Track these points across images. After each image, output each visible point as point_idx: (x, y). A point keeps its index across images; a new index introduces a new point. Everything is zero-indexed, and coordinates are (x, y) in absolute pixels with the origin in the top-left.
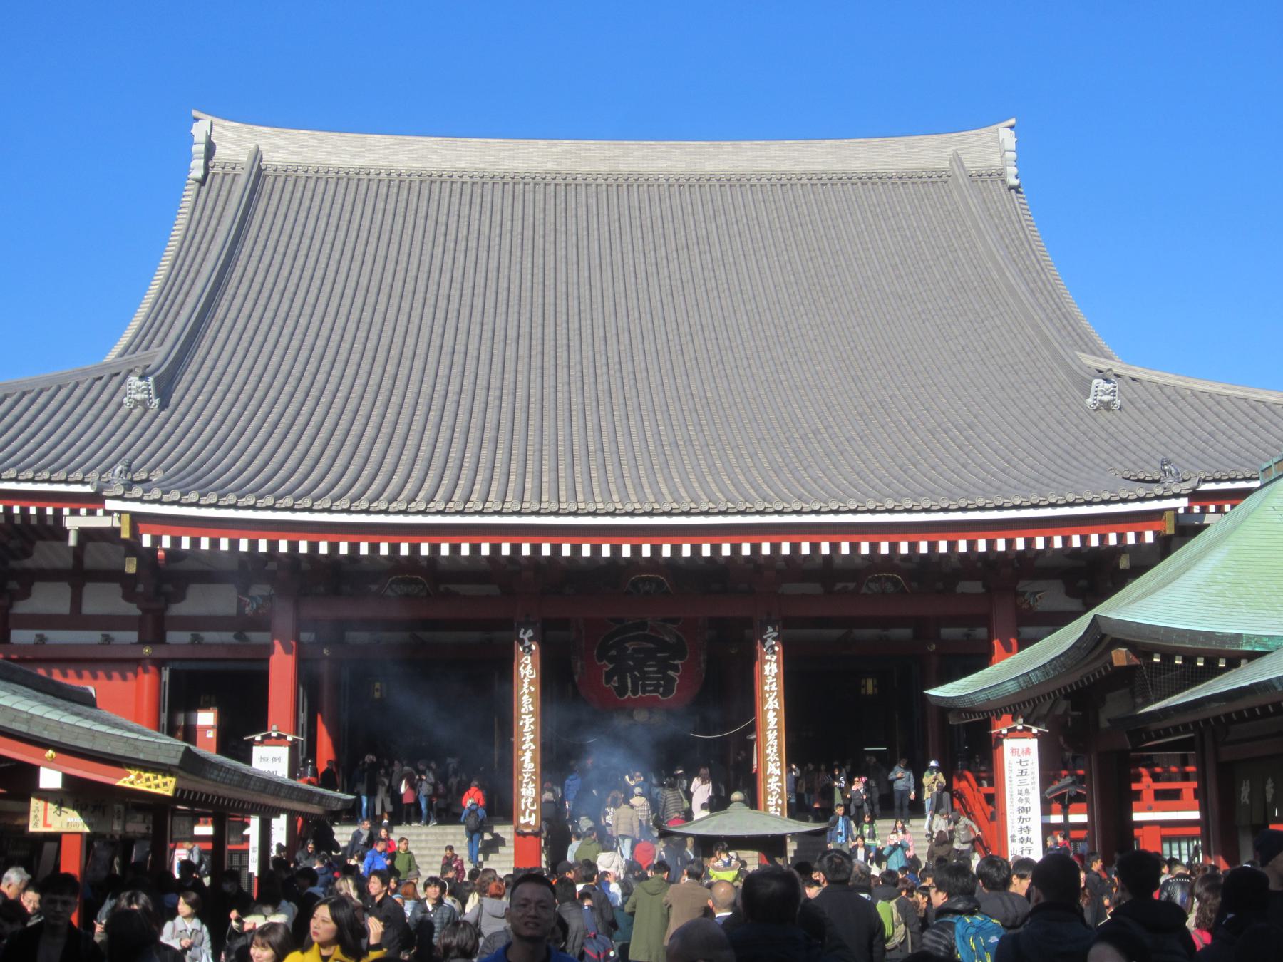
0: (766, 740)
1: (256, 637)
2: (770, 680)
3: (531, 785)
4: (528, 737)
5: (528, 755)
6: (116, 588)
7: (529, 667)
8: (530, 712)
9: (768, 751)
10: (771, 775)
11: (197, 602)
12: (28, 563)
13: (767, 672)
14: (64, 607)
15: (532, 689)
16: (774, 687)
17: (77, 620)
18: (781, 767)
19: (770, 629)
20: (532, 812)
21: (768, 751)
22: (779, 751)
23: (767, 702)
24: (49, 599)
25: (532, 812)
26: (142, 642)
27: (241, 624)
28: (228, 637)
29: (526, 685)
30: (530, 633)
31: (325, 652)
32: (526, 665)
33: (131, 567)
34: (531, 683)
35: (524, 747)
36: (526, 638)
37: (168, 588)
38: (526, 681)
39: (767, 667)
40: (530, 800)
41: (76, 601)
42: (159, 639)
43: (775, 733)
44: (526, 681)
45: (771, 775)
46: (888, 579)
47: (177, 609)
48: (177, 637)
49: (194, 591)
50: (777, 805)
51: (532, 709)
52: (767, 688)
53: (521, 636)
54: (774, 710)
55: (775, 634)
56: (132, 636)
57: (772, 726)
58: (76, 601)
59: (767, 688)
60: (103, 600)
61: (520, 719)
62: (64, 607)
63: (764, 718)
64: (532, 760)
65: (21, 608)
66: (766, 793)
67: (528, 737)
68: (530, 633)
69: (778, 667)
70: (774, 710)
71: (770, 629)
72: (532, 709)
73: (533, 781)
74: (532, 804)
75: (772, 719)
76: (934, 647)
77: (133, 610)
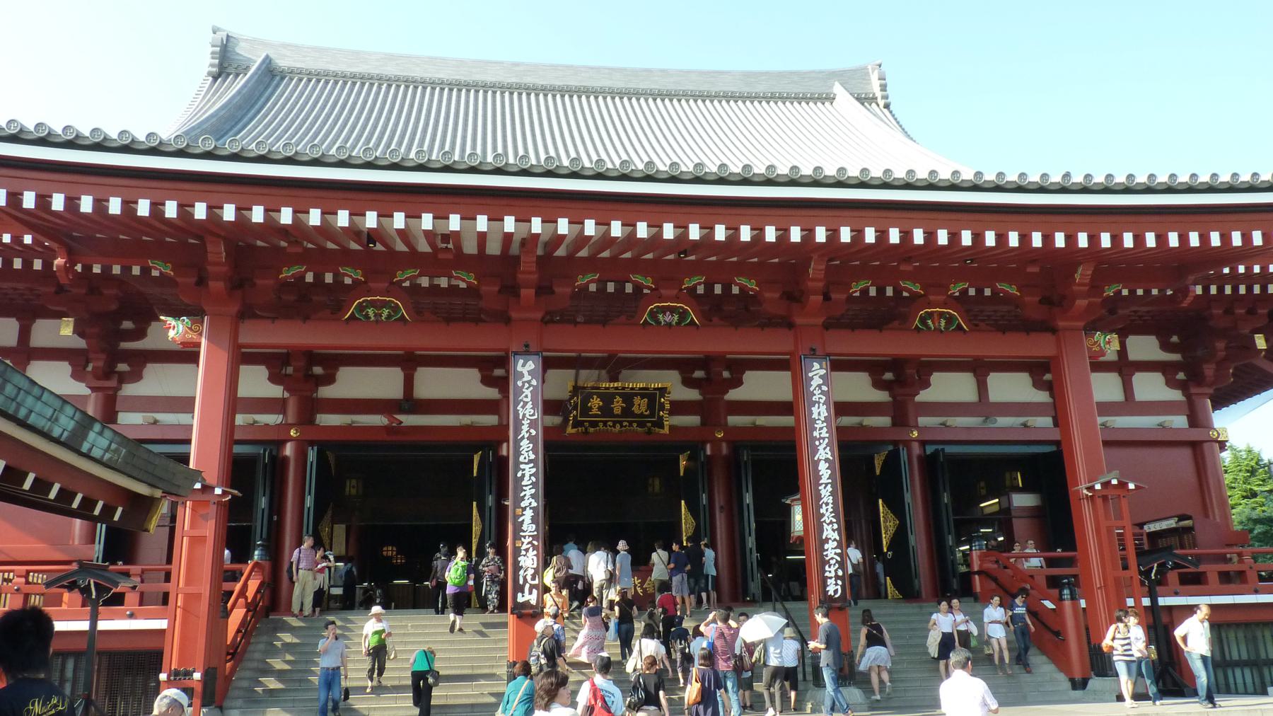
0: (819, 497)
2: (819, 425)
3: (532, 553)
4: (529, 491)
5: (529, 514)
7: (529, 405)
8: (530, 461)
9: (823, 511)
10: (827, 540)
13: (815, 416)
15: (533, 432)
16: (825, 434)
18: (839, 530)
19: (816, 365)
20: (532, 587)
21: (823, 511)
22: (835, 510)
23: (816, 450)
25: (532, 587)
29: (525, 428)
30: (531, 365)
31: (292, 433)
32: (526, 403)
34: (533, 424)
35: (523, 505)
36: (525, 371)
37: (123, 367)
38: (526, 422)
39: (815, 410)
40: (531, 572)
43: (829, 488)
44: (526, 422)
45: (827, 540)
46: (941, 315)
50: (837, 577)
51: (532, 457)
52: (816, 434)
53: (519, 368)
54: (826, 460)
55: (823, 372)
57: (824, 480)
59: (816, 434)
61: (517, 469)
63: (817, 471)
64: (534, 520)
66: (824, 562)
67: (529, 491)
68: (531, 365)
69: (828, 410)
70: (826, 460)
71: (816, 365)
72: (532, 457)
73: (535, 548)
74: (533, 579)
75: (824, 469)
76: (915, 434)
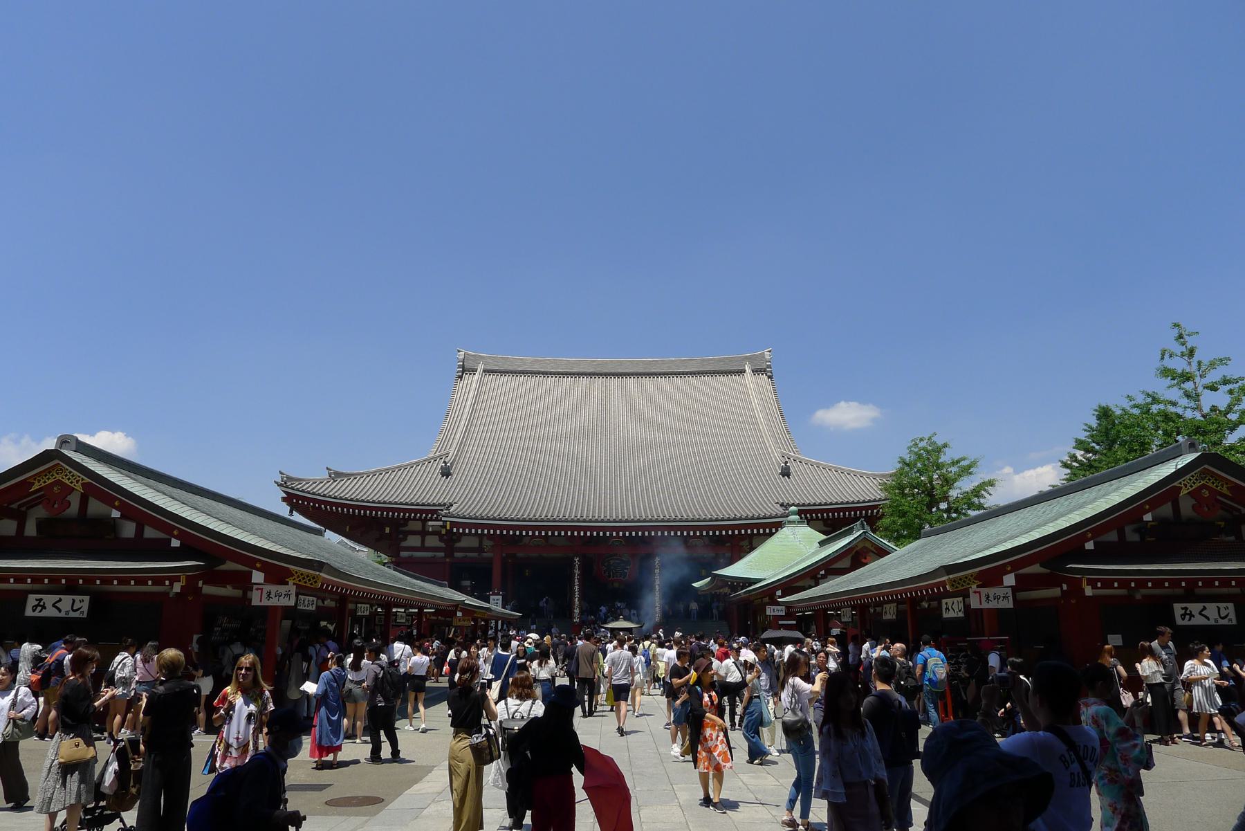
1: (485, 555)
6: (437, 537)
11: (464, 543)
12: (406, 529)
14: (419, 544)
17: (423, 548)
24: (413, 541)
26: (446, 556)
27: (480, 549)
28: (475, 555)
33: (444, 532)
41: (423, 541)
42: (452, 555)
47: (458, 545)
48: (457, 555)
49: (464, 538)
56: (442, 554)
58: (423, 541)
60: (432, 541)
62: (419, 544)
65: (404, 544)
77: (442, 545)
